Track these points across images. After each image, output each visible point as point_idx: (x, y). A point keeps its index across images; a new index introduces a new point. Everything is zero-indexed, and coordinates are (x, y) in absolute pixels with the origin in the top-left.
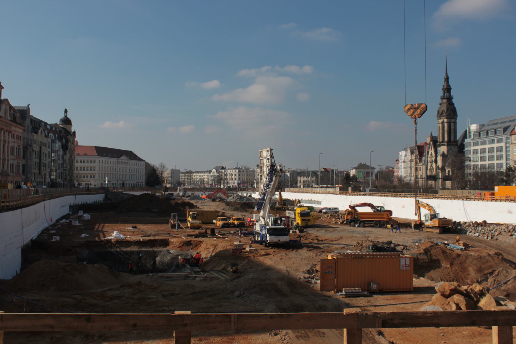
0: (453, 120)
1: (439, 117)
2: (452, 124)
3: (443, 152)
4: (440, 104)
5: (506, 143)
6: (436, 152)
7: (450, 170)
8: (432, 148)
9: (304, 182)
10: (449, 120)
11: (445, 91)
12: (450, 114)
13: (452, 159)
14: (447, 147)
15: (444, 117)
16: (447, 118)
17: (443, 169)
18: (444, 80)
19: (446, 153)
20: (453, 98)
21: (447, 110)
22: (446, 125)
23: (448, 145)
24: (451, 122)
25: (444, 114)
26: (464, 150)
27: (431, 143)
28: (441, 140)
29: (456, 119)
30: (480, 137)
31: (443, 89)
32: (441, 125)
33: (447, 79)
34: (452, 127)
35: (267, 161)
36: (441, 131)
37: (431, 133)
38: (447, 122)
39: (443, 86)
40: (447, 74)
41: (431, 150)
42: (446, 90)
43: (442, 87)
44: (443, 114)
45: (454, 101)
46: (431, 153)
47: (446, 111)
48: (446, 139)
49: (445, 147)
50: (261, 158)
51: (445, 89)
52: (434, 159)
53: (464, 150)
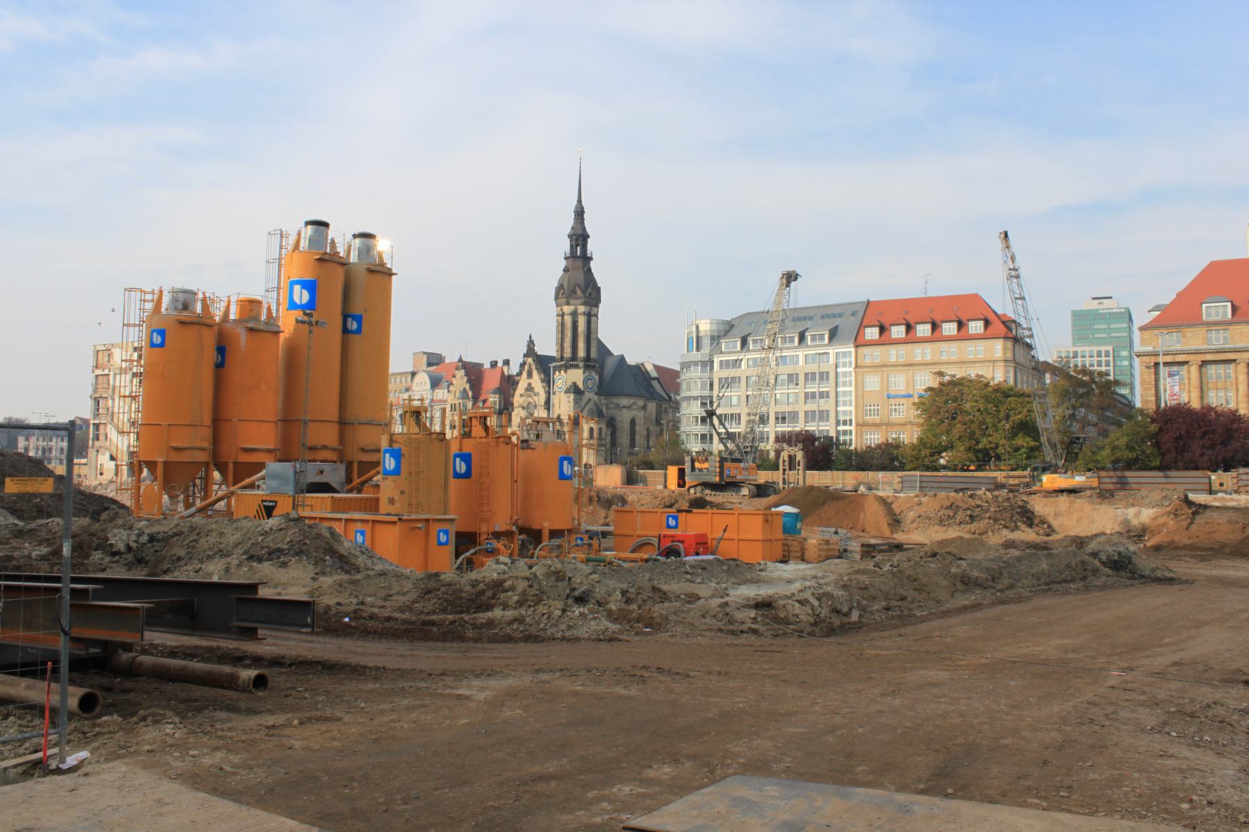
0: (594, 310)
1: (564, 300)
2: (593, 319)
3: (575, 384)
4: (566, 270)
5: (837, 366)
6: (548, 381)
7: (593, 426)
8: (535, 373)
9: (43, 449)
10: (588, 308)
11: (577, 239)
12: (590, 294)
13: (595, 402)
14: (584, 373)
15: (580, 301)
16: (585, 304)
17: (576, 422)
18: (573, 216)
19: (581, 386)
20: (591, 259)
21: (587, 286)
22: (582, 321)
23: (587, 367)
24: (592, 313)
25: (579, 292)
26: (678, 381)
27: (530, 360)
28: (568, 353)
29: (597, 306)
30: (744, 350)
31: (570, 236)
32: (568, 319)
33: (580, 213)
34: (593, 326)
35: (132, 382)
36: (569, 333)
37: (530, 337)
38: (584, 314)
39: (573, 228)
40: (580, 201)
41: (530, 375)
42: (580, 239)
43: (569, 231)
44: (575, 292)
45: (592, 264)
46: (529, 384)
47: (583, 286)
48: (581, 353)
49: (581, 371)
50: (98, 372)
51: (580, 235)
52: (541, 399)
53: (678, 381)
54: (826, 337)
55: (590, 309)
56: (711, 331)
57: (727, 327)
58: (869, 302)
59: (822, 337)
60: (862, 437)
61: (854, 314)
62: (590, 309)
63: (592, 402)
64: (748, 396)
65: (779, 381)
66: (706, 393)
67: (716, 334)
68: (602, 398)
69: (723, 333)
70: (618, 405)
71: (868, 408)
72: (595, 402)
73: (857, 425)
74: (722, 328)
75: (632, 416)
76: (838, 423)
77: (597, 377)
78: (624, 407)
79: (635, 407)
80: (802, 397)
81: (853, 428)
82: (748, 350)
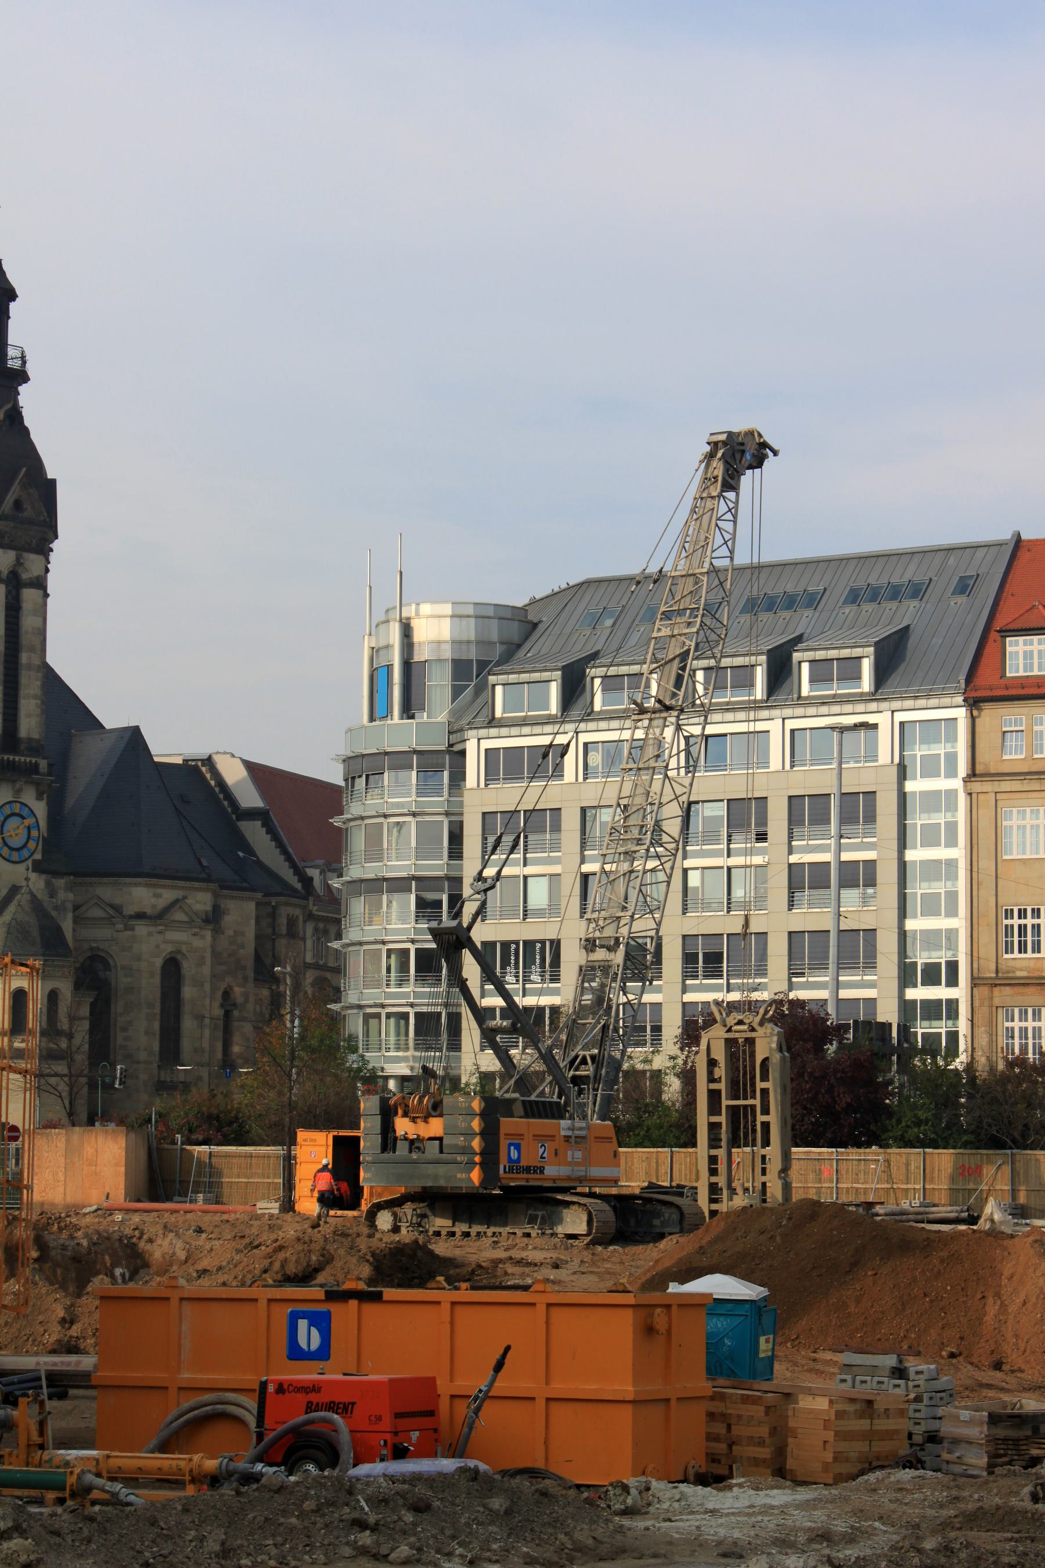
0: (33, 561)
2: (29, 595)
5: (902, 772)
12: (18, 505)
13: (36, 904)
20: (21, 376)
24: (25, 576)
26: (337, 821)
29: (44, 550)
30: (576, 712)
34: (28, 622)
53: (337, 821)
54: (867, 667)
55: (19, 562)
56: (455, 643)
57: (514, 631)
58: (1018, 542)
59: (850, 670)
60: (992, 1025)
61: (964, 587)
62: (19, 562)
63: (22, 898)
64: (585, 878)
65: (697, 825)
66: (437, 866)
67: (473, 654)
68: (60, 883)
69: (499, 650)
70: (117, 909)
71: (1016, 922)
72: (36, 904)
73: (976, 982)
74: (495, 637)
75: (170, 948)
76: (906, 975)
77: (40, 809)
78: (141, 916)
79: (179, 916)
80: (779, 881)
81: (960, 993)
82: (589, 715)
